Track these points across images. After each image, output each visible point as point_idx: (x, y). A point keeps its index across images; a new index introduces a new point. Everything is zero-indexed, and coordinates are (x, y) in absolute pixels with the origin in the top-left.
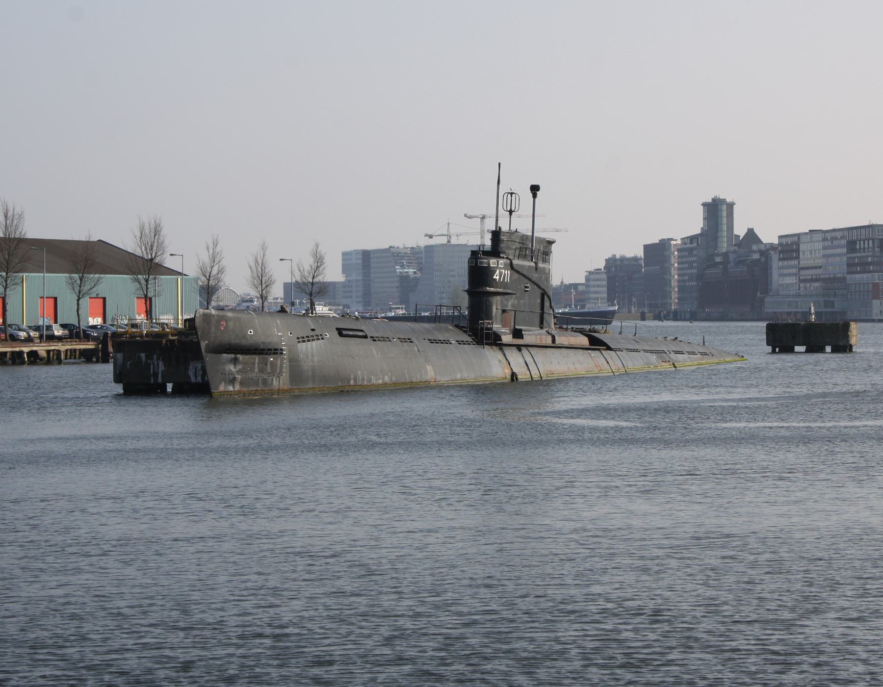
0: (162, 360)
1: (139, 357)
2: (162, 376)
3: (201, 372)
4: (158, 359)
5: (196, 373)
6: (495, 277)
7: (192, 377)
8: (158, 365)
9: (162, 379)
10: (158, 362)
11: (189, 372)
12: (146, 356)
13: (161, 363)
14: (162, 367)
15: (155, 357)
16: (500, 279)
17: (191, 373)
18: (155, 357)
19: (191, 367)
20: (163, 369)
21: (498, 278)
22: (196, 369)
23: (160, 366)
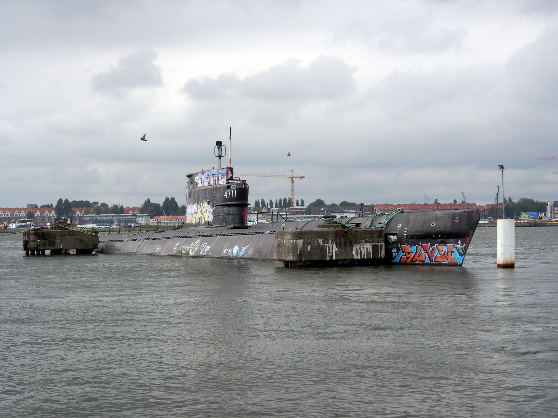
0: (335, 244)
1: (318, 241)
2: (336, 255)
3: (360, 252)
4: (332, 243)
5: (357, 252)
6: (225, 196)
7: (355, 255)
8: (332, 247)
9: (336, 257)
10: (332, 245)
11: (353, 252)
12: (323, 241)
13: (335, 246)
14: (335, 248)
15: (330, 242)
16: (228, 196)
17: (354, 252)
18: (330, 242)
19: (354, 248)
20: (336, 250)
21: (226, 196)
22: (357, 249)
23: (334, 248)
